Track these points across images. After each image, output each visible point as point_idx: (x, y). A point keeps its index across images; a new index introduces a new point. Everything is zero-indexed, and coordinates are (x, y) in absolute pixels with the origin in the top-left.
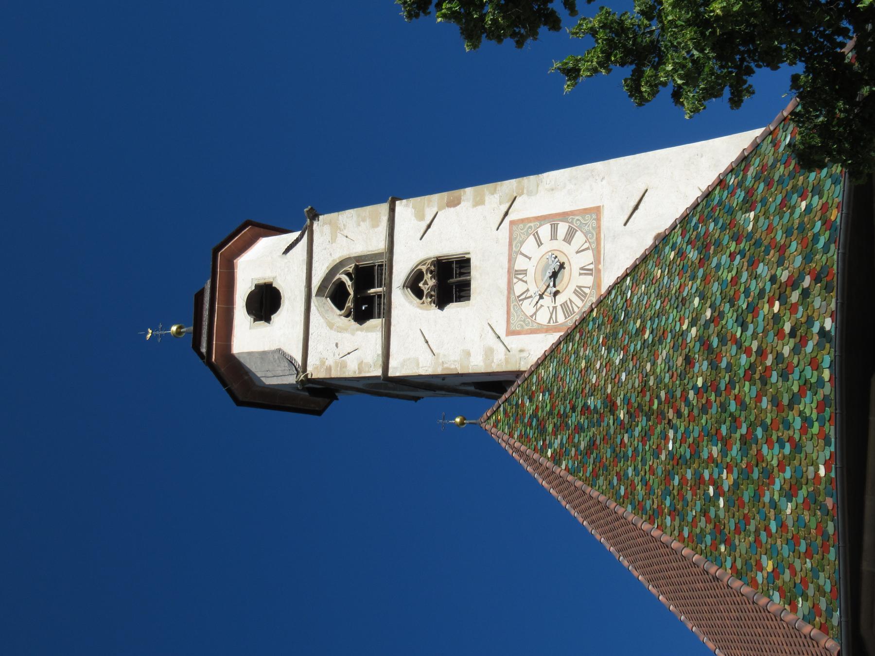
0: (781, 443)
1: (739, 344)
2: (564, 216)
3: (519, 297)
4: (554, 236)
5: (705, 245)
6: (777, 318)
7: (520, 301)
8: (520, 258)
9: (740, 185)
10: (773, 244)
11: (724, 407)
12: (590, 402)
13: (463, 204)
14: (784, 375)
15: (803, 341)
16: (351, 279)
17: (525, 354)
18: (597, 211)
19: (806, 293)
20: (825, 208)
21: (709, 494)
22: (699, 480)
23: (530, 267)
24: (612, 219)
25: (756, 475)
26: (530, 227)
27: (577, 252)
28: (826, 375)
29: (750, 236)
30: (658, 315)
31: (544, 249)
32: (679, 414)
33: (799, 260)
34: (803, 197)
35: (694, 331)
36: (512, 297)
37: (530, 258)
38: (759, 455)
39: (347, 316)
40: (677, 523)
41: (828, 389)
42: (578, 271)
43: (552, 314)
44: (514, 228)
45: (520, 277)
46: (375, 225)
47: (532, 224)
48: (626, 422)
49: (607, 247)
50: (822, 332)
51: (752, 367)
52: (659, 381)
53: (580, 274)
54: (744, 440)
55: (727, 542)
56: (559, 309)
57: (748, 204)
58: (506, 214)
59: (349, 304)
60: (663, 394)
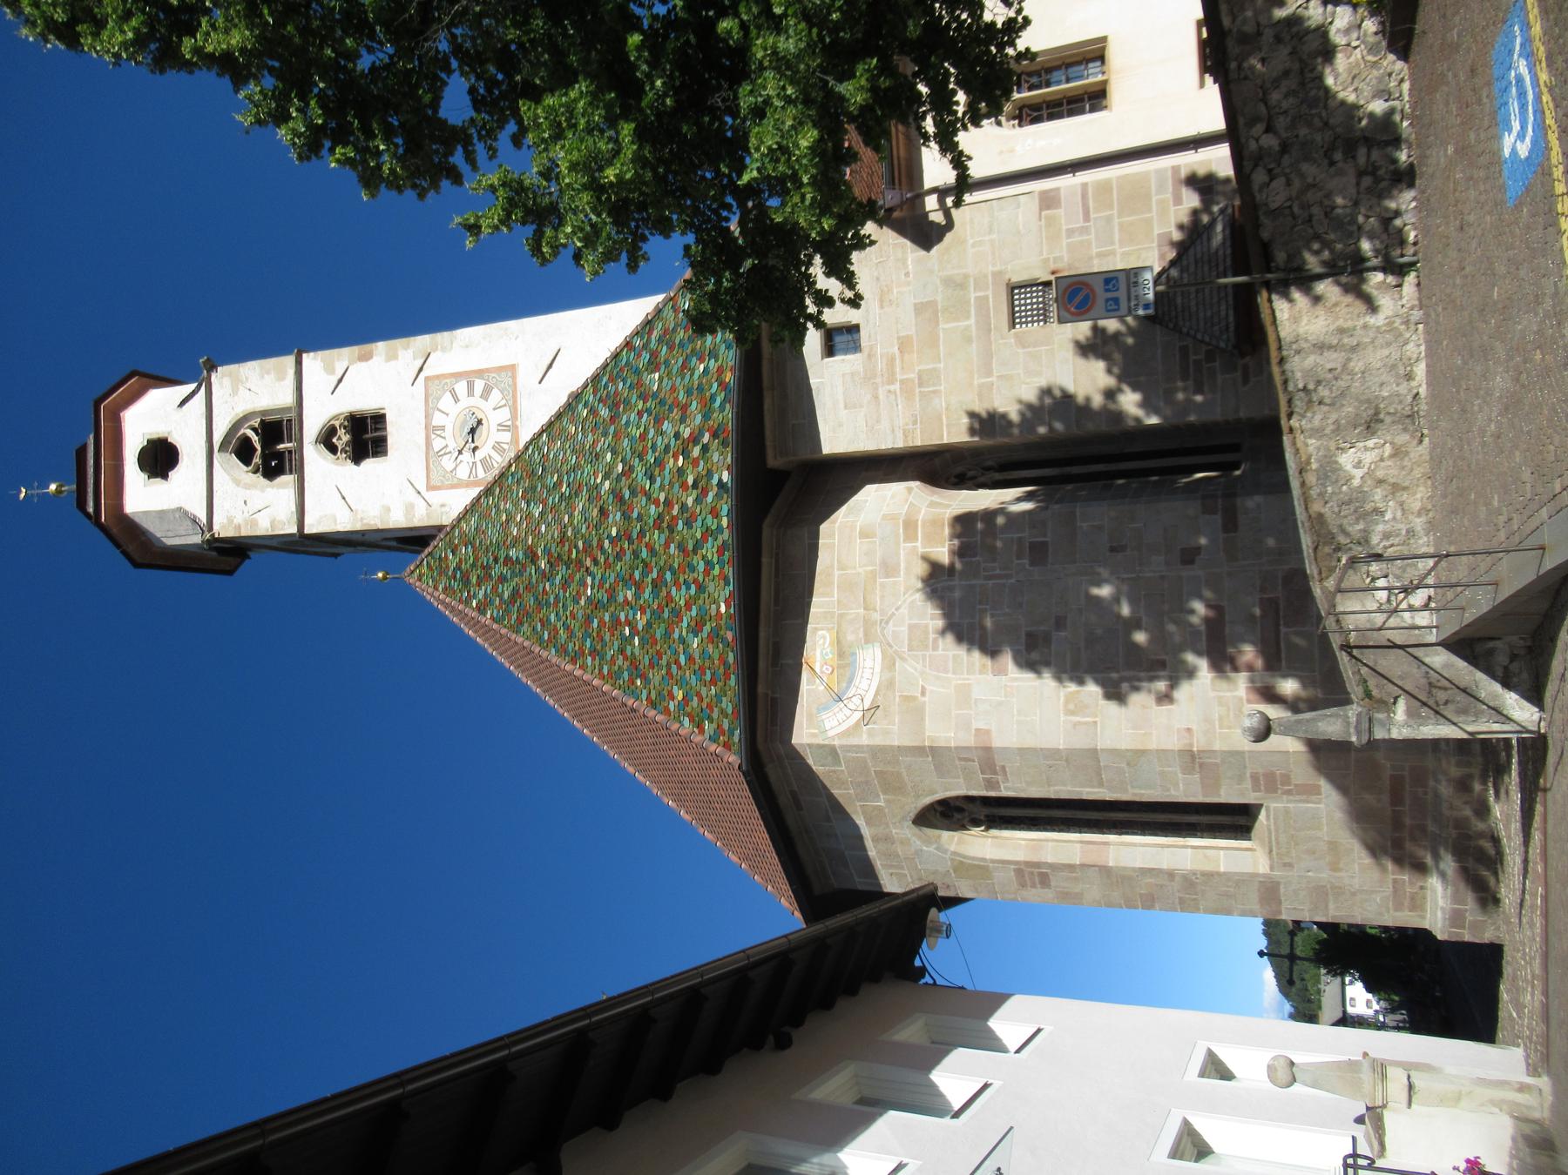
1: (648, 495)
2: (480, 373)
4: (471, 392)
5: (615, 403)
6: (681, 472)
8: (437, 415)
9: (645, 346)
10: (676, 403)
11: (636, 554)
12: (512, 553)
13: (375, 358)
14: (689, 524)
15: (705, 492)
16: (257, 434)
17: (447, 509)
18: (512, 368)
19: (705, 449)
20: (720, 370)
22: (618, 621)
24: (527, 377)
25: (666, 615)
26: (446, 383)
27: (494, 409)
28: (725, 522)
29: (655, 395)
31: (461, 405)
32: (595, 562)
33: (699, 417)
34: (701, 360)
35: (607, 484)
36: (431, 452)
38: (669, 598)
39: (256, 472)
40: (597, 662)
41: (726, 535)
42: (496, 427)
45: (438, 432)
46: (281, 378)
47: (448, 381)
49: (524, 404)
50: (721, 484)
51: (660, 517)
52: (576, 532)
54: (655, 584)
55: (644, 677)
56: (479, 464)
57: (653, 365)
58: (421, 369)
59: (257, 460)
60: (580, 544)
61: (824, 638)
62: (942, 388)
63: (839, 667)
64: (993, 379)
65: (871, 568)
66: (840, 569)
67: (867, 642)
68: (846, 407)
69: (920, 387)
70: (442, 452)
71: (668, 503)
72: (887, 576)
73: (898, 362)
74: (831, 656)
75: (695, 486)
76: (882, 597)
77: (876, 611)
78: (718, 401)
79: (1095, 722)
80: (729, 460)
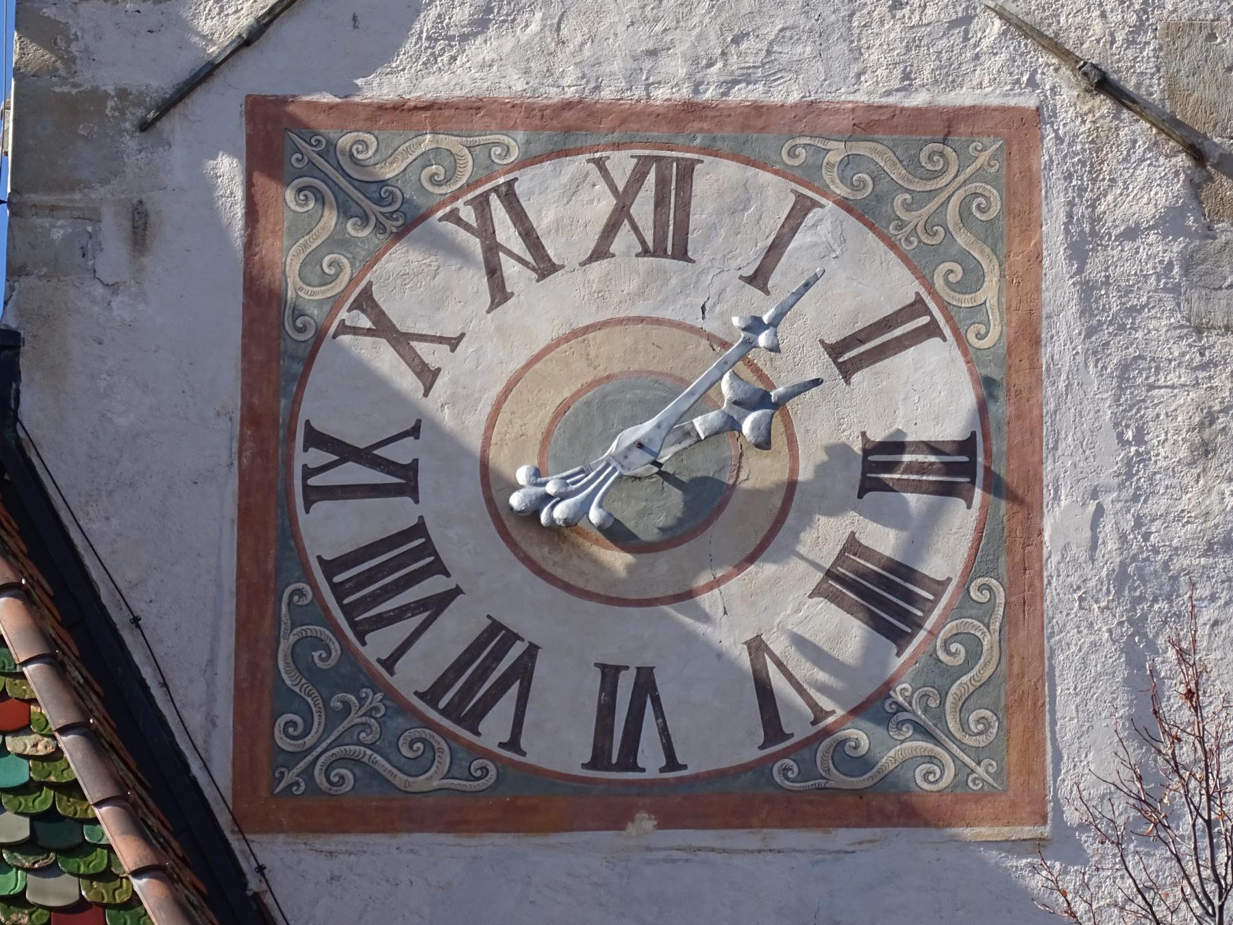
7: (481, 205)
26: (972, 280)
36: (515, 144)
43: (365, 456)
45: (643, 208)
47: (989, 293)
53: (610, 674)
70: (506, 233)
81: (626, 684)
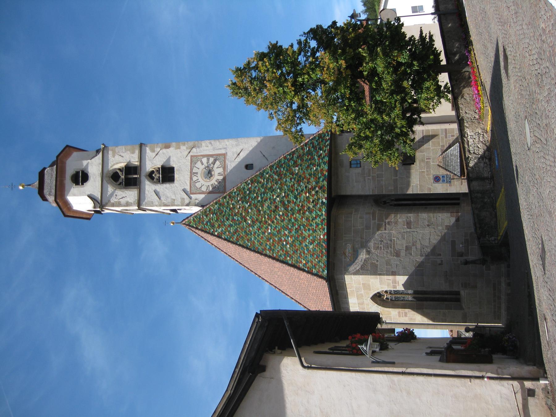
0: (309, 230)
1: (295, 203)
2: (212, 156)
3: (195, 181)
5: (280, 175)
7: (195, 183)
8: (195, 168)
10: (305, 177)
11: (290, 220)
14: (311, 212)
15: (317, 204)
18: (224, 155)
19: (317, 192)
20: (322, 170)
21: (284, 244)
22: (281, 240)
23: (199, 172)
25: (300, 238)
26: (199, 158)
27: (217, 168)
28: (324, 213)
29: (297, 174)
30: (264, 193)
32: (273, 222)
33: (314, 183)
35: (278, 199)
36: (192, 181)
37: (199, 169)
38: (302, 233)
43: (207, 188)
44: (193, 158)
45: (195, 175)
46: (133, 153)
47: (200, 157)
48: (251, 224)
51: (300, 210)
52: (265, 212)
53: (218, 175)
55: (290, 256)
56: (210, 186)
57: (296, 165)
58: (189, 152)
59: (120, 181)
60: (266, 216)
61: (349, 246)
62: (384, 179)
63: (353, 254)
64: (398, 178)
65: (362, 227)
66: (354, 227)
67: (361, 248)
68: (356, 182)
69: (377, 178)
71: (302, 206)
72: (367, 229)
73: (371, 171)
74: (351, 251)
75: (313, 202)
76: (366, 235)
77: (364, 239)
78: (321, 179)
79: (423, 270)
80: (326, 195)
81: (219, 174)
